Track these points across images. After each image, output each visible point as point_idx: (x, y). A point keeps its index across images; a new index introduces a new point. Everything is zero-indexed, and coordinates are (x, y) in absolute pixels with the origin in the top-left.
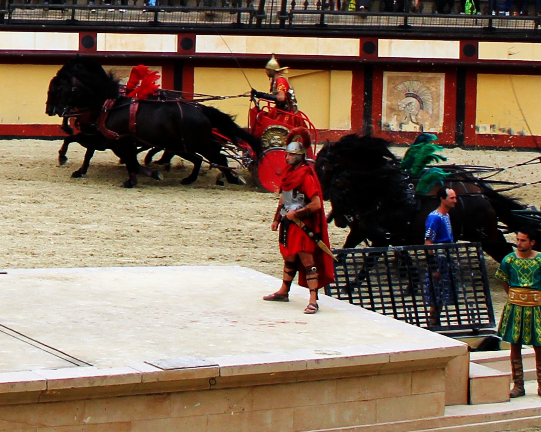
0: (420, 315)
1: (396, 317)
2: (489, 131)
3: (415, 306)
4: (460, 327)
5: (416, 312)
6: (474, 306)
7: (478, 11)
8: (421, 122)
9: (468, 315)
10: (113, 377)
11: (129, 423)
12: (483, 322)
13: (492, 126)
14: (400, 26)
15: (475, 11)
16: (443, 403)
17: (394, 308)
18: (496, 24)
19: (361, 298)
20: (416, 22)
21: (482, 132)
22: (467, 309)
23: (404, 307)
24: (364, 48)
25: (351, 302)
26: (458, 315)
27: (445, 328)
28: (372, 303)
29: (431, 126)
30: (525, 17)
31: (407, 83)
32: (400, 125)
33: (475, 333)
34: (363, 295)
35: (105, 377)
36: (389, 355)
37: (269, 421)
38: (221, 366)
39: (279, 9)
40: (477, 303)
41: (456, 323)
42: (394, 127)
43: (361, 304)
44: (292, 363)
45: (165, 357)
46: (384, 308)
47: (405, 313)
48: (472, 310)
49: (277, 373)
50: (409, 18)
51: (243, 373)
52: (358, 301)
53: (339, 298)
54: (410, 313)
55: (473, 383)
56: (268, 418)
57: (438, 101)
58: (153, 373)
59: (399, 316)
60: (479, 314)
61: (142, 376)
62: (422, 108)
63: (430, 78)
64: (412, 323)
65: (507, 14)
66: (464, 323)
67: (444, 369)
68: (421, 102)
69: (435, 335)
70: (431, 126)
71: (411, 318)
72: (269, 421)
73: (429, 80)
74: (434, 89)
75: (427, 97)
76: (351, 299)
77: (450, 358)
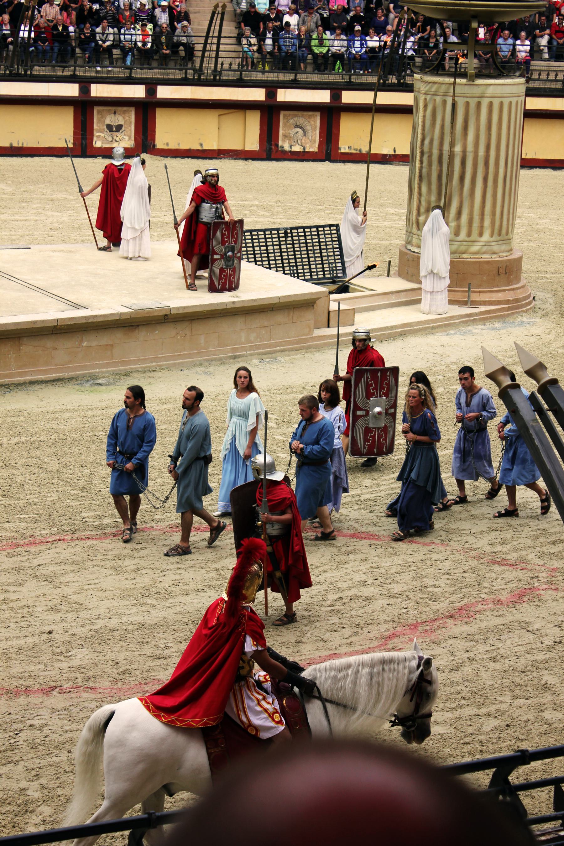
0: (299, 271)
1: (284, 273)
2: (347, 151)
3: (297, 266)
4: (325, 278)
5: (297, 270)
6: (334, 265)
7: (343, 70)
8: (304, 145)
9: (330, 271)
10: (101, 316)
11: (112, 345)
12: (339, 275)
13: (350, 147)
14: (292, 80)
15: (341, 71)
16: (312, 326)
17: (283, 267)
18: (354, 79)
19: (262, 261)
20: (302, 77)
21: (343, 151)
22: (329, 267)
23: (290, 266)
24: (268, 95)
25: (256, 264)
26: (324, 271)
27: (315, 279)
28: (269, 264)
29: (311, 147)
30: (370, 74)
31: (296, 119)
32: (291, 147)
33: (334, 282)
34: (264, 259)
35: (96, 316)
36: (279, 298)
37: (202, 341)
38: (172, 306)
39: (213, 68)
40: (336, 263)
41: (322, 276)
42: (287, 148)
43: (262, 265)
44: (217, 304)
45: (136, 302)
46: (276, 267)
47: (290, 270)
48: (332, 268)
49: (207, 311)
50: (298, 76)
51: (185, 311)
52: (260, 263)
53: (248, 261)
54: (293, 271)
55: (331, 314)
56: (202, 339)
57: (315, 131)
58: (127, 313)
59: (286, 272)
60: (337, 270)
61: (121, 314)
62: (305, 135)
63: (311, 115)
64: (294, 277)
65: (361, 72)
66: (327, 276)
67: (313, 306)
68: (305, 132)
69: (309, 284)
70: (311, 147)
71: (294, 273)
72: (202, 341)
73: (310, 117)
74: (312, 123)
75: (309, 128)
76: (256, 262)
77: (318, 299)
